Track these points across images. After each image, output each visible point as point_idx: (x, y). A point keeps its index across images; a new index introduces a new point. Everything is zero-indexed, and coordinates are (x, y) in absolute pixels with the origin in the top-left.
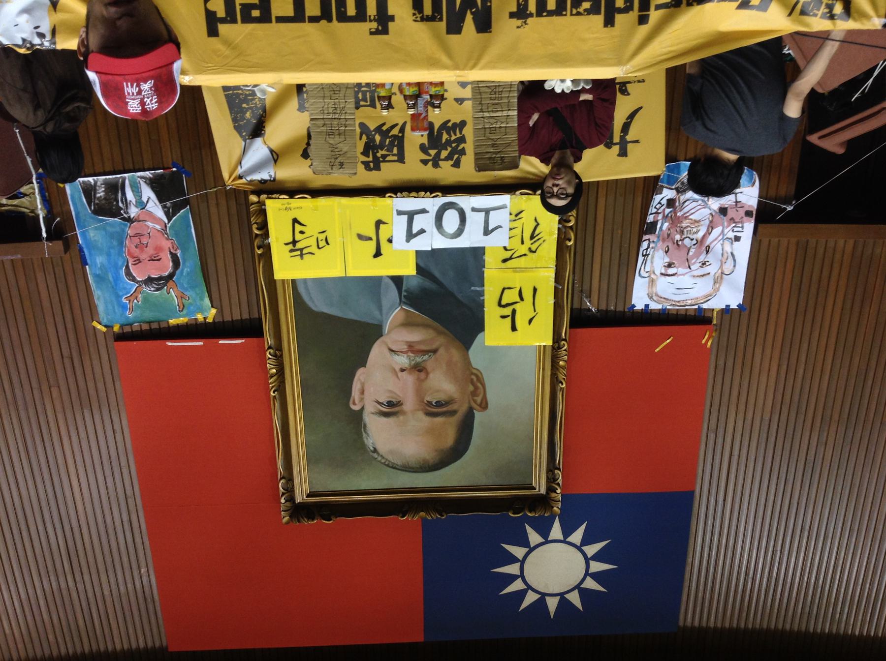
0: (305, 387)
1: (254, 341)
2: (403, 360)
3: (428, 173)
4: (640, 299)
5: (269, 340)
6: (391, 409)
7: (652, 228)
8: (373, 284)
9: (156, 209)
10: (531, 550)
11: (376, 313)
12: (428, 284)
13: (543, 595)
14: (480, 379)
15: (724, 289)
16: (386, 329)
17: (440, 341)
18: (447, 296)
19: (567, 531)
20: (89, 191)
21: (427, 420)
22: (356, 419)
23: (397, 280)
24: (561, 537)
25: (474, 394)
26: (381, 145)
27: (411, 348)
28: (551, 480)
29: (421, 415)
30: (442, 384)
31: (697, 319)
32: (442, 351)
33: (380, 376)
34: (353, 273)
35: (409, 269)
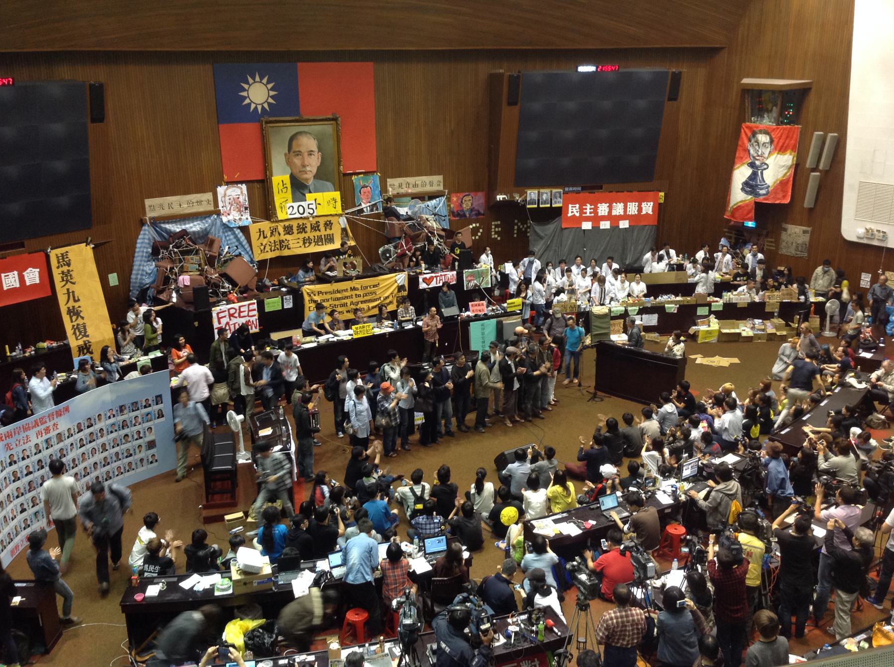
2: (308, 169)
3: (305, 221)
4: (244, 187)
6: (310, 153)
7: (246, 208)
8: (316, 191)
9: (363, 206)
15: (223, 193)
18: (299, 188)
19: (256, 108)
20: (377, 209)
22: (320, 149)
23: (310, 192)
26: (316, 227)
30: (297, 161)
31: (228, 183)
33: (313, 163)
34: (320, 194)
35: (308, 195)
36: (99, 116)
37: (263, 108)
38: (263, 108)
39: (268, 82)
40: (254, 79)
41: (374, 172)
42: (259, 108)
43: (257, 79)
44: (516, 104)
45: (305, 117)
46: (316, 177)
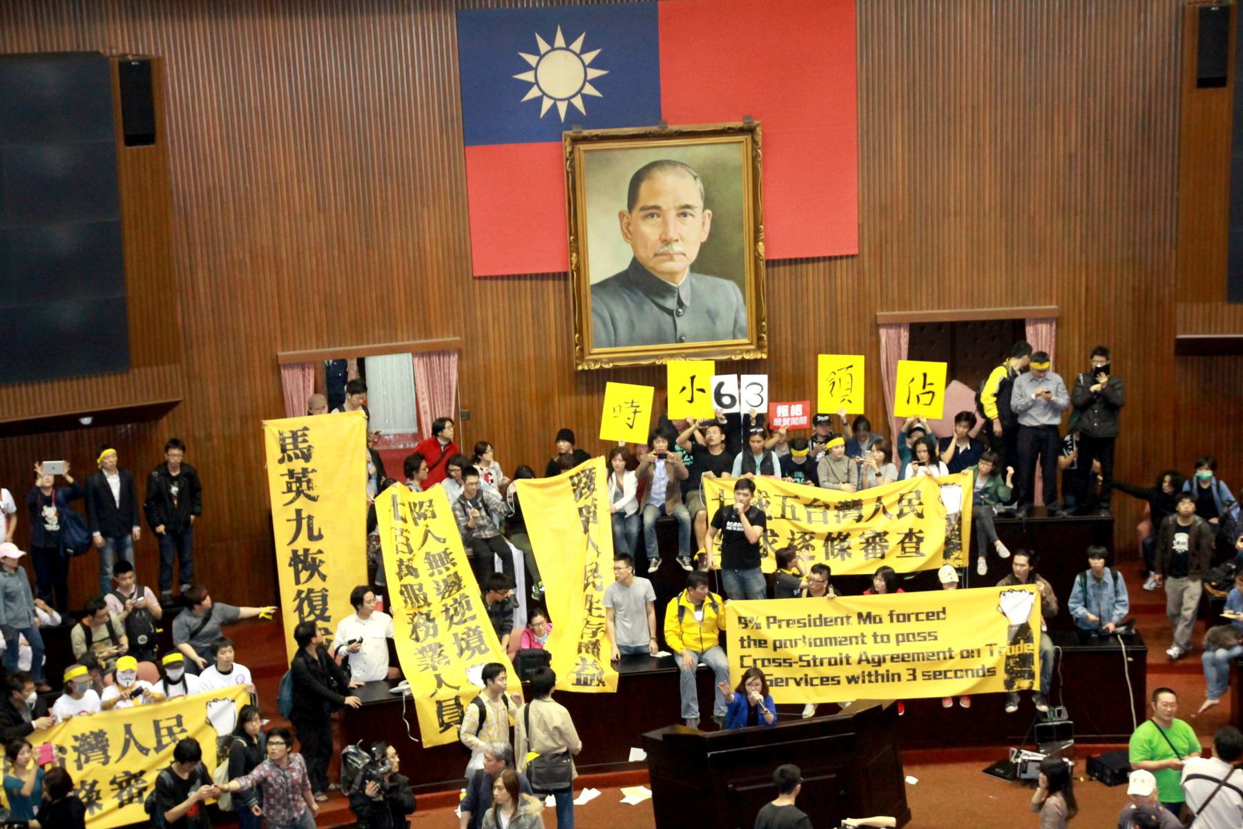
0: (741, 226)
1: (771, 257)
2: (676, 248)
5: (762, 264)
6: (684, 211)
10: (579, 92)
11: (694, 281)
12: (660, 301)
13: (567, 49)
14: (625, 235)
16: (688, 269)
17: (650, 263)
19: (554, 109)
21: (660, 203)
22: (708, 202)
24: (559, 103)
25: (629, 224)
27: (671, 257)
28: (573, 160)
29: (664, 207)
30: (650, 230)
32: (651, 255)
33: (691, 235)
36: (143, 130)
37: (571, 107)
38: (571, 107)
39: (585, 49)
40: (550, 40)
41: (853, 256)
42: (562, 108)
43: (560, 41)
44: (1220, 82)
45: (673, 128)
46: (696, 268)
